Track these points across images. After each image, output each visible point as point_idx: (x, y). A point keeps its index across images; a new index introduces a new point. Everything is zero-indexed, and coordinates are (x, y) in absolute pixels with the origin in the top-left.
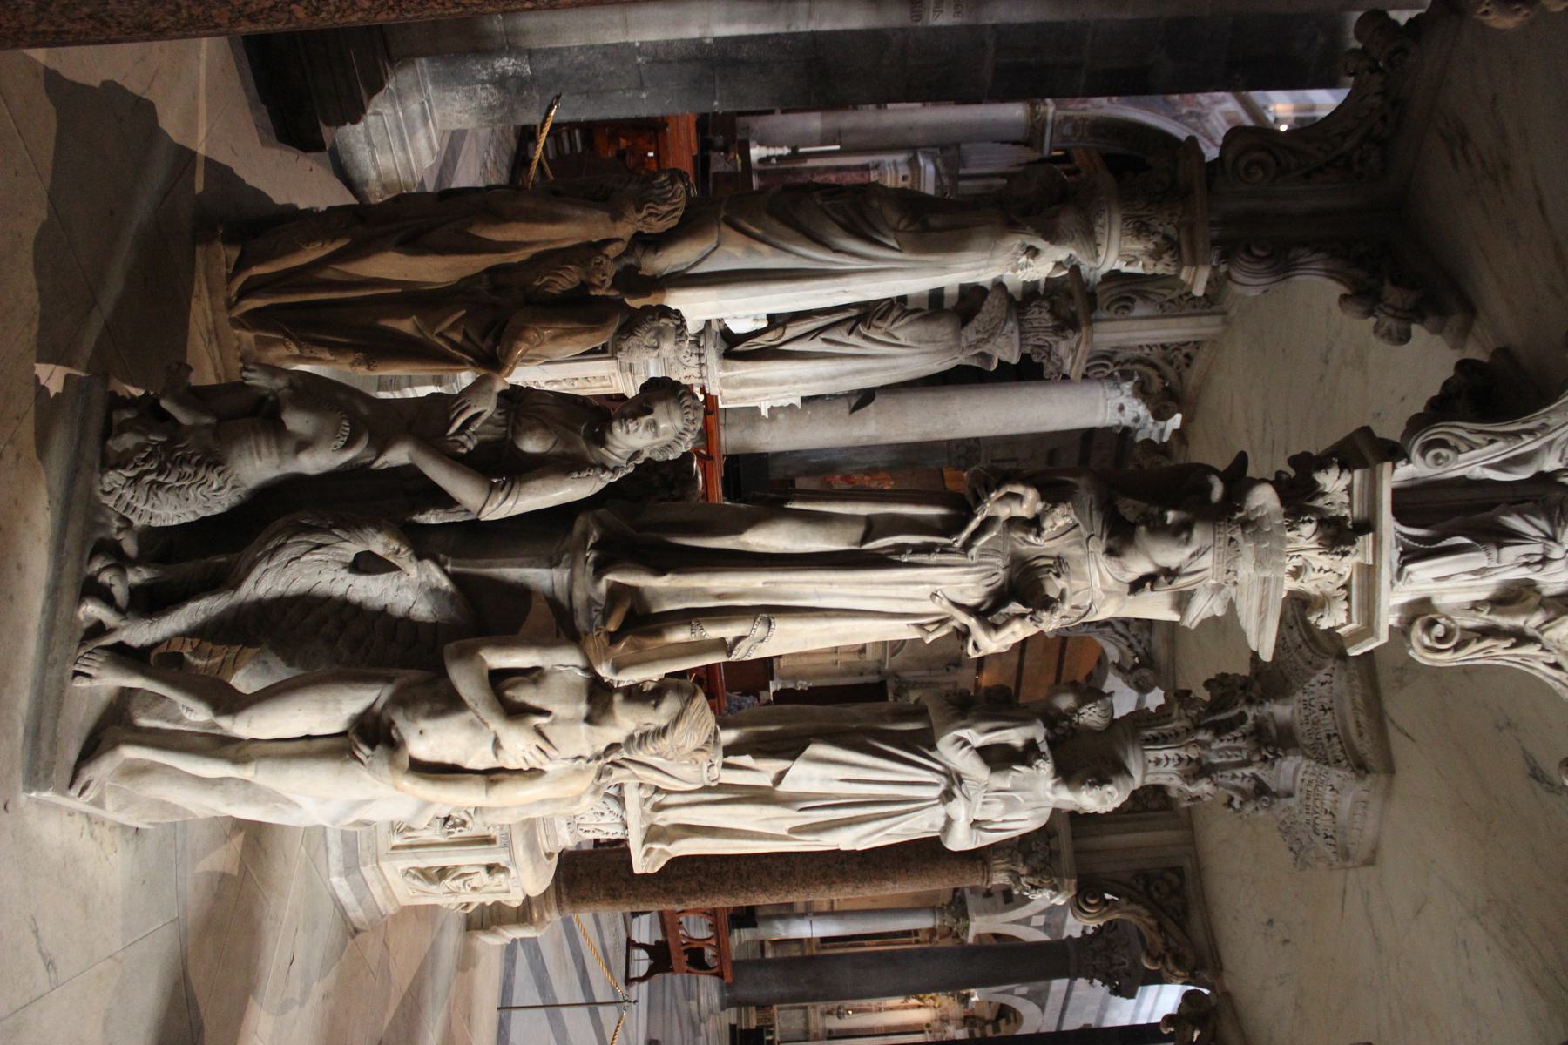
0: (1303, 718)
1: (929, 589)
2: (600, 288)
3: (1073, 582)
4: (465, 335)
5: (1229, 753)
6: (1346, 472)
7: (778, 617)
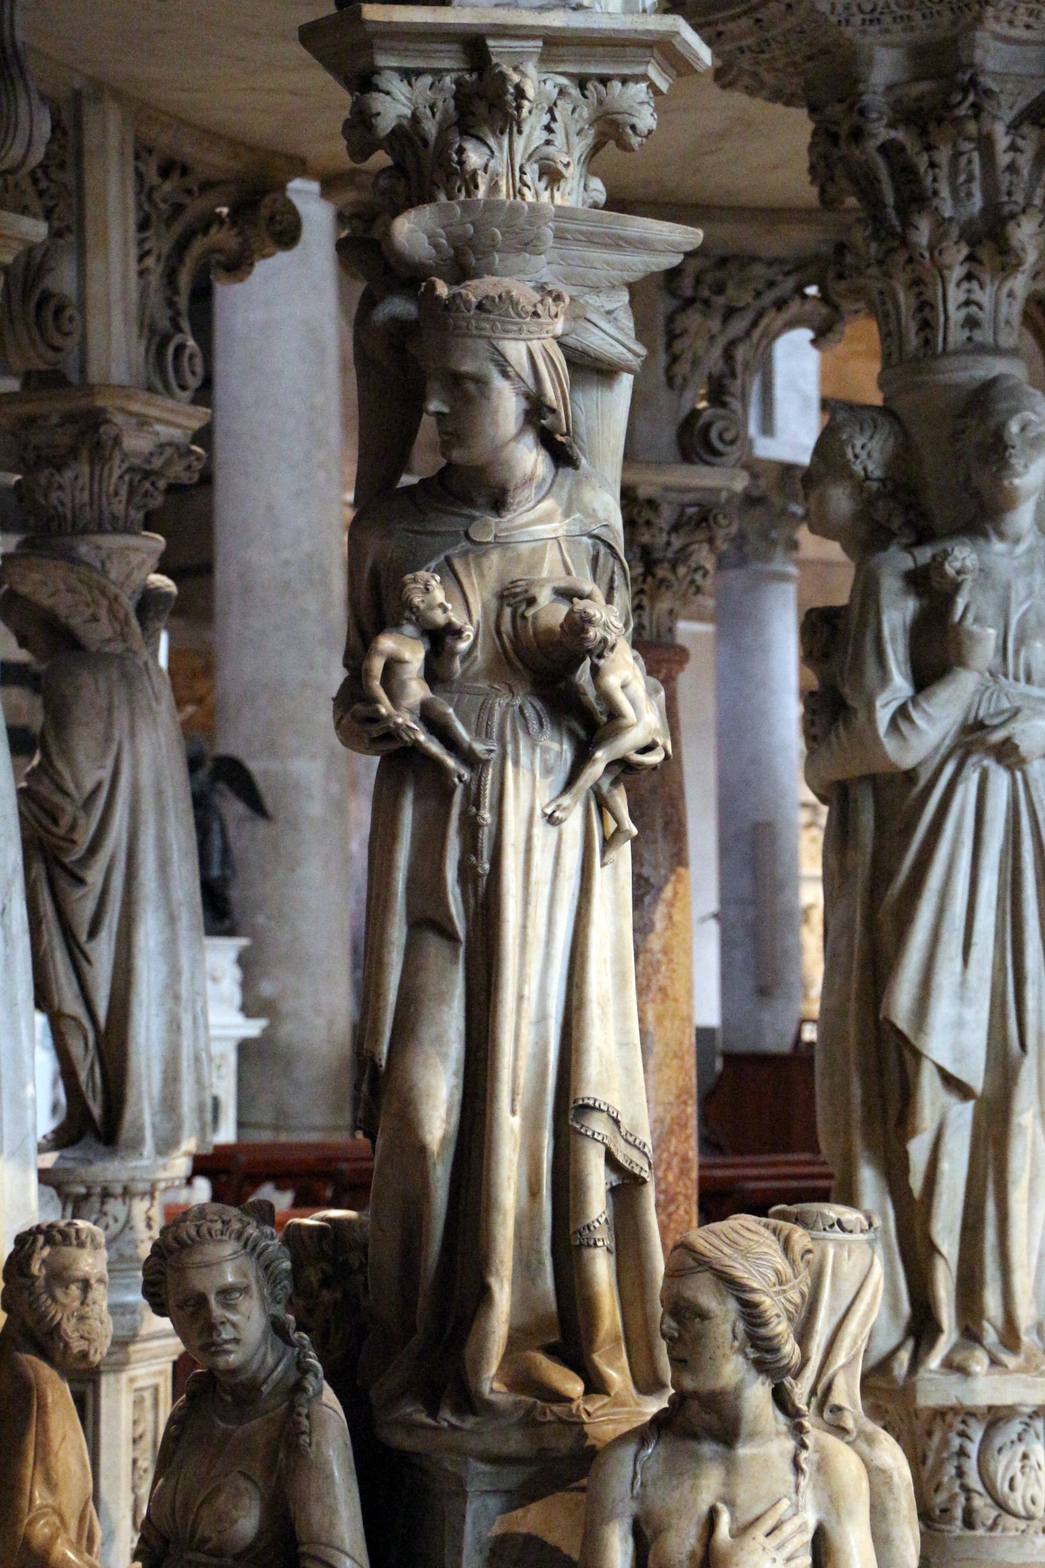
0: (899, 27)
1: (540, 828)
3: (545, 574)
5: (962, 178)
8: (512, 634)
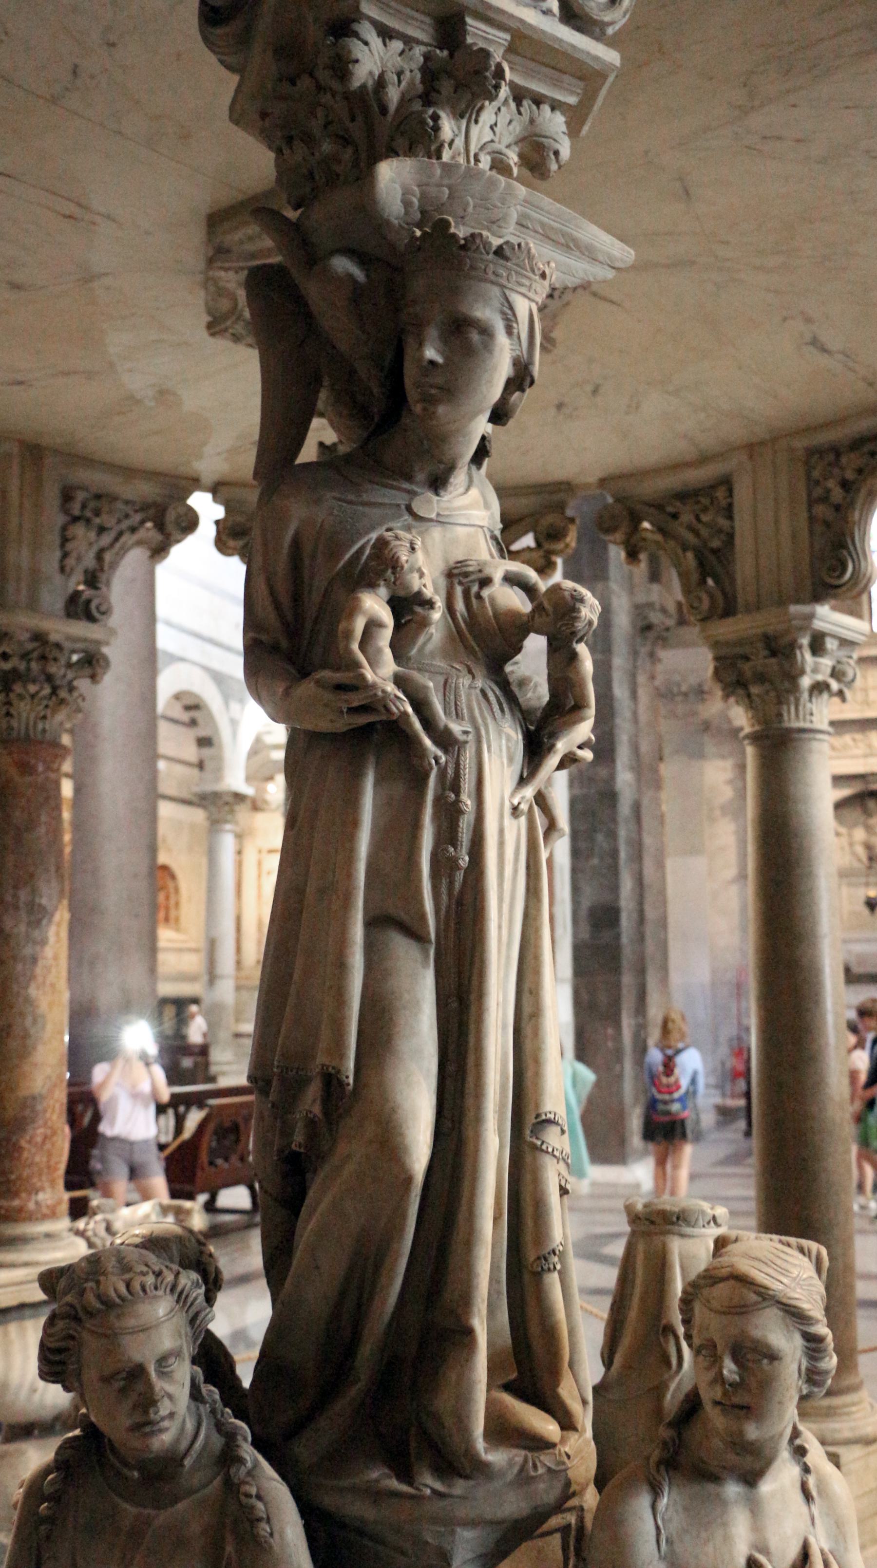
1: (508, 820)
6: (356, 27)
7: (537, 1105)
8: (466, 614)
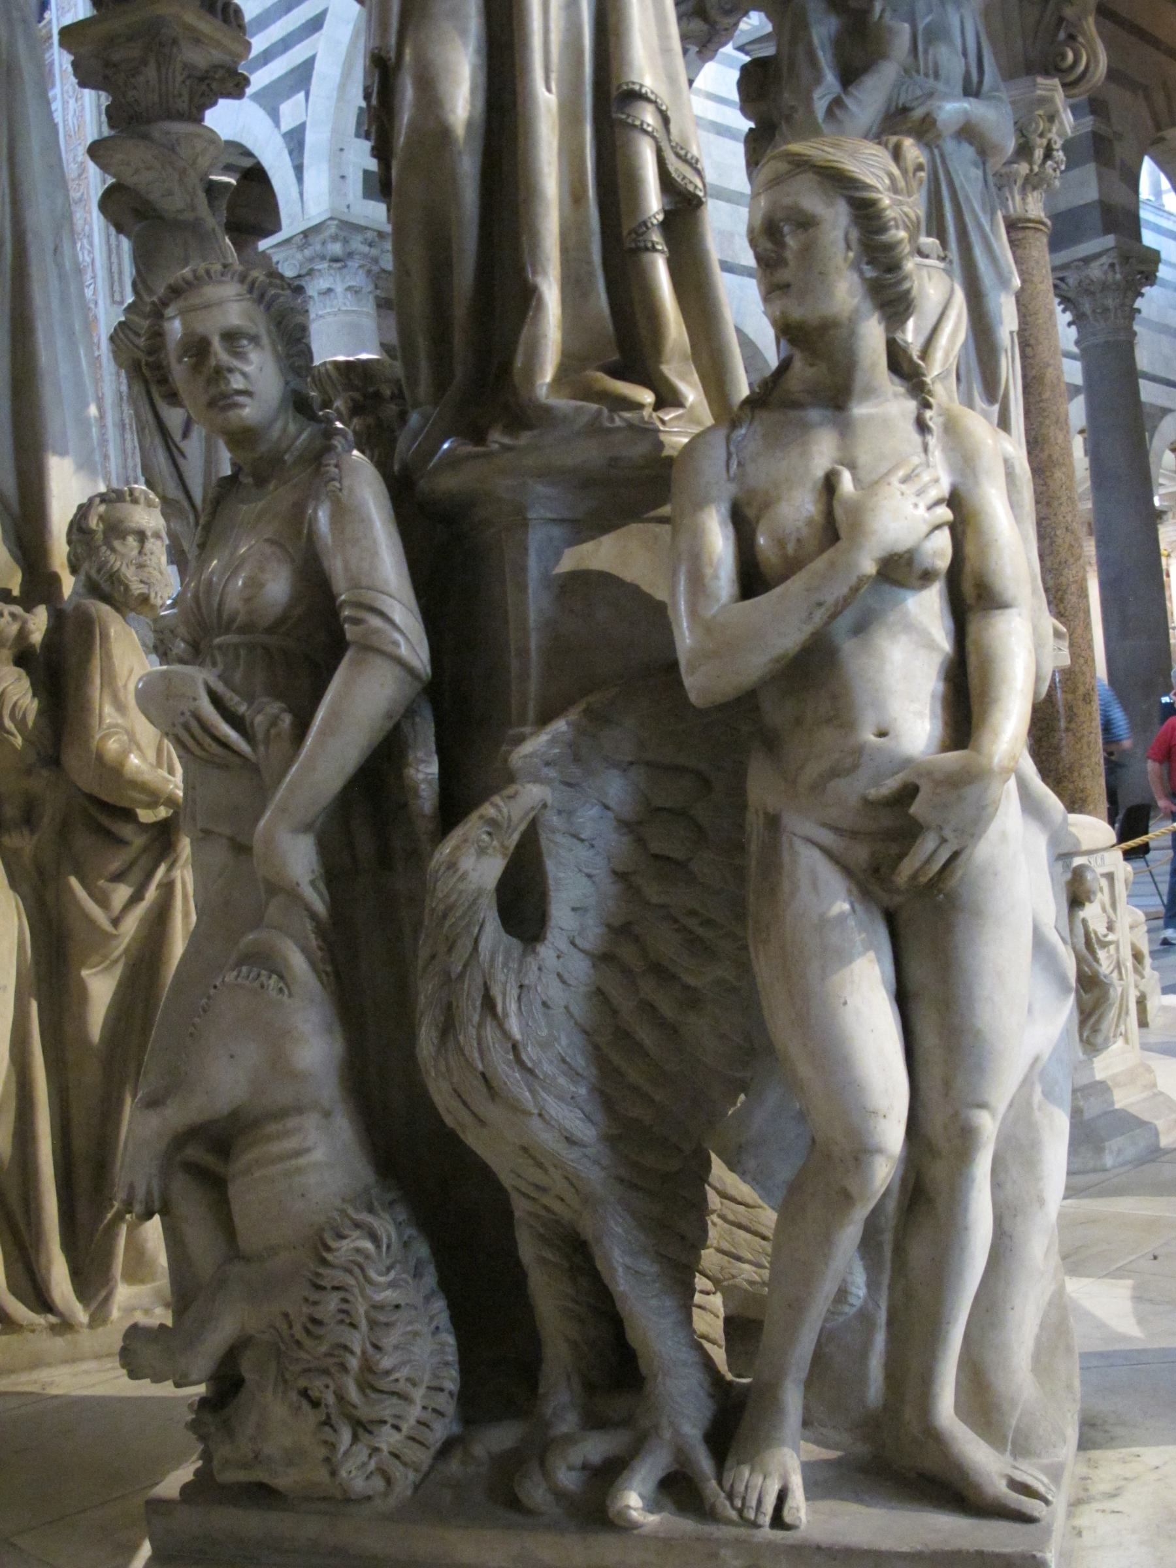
2: (25, 622)
4: (118, 877)
